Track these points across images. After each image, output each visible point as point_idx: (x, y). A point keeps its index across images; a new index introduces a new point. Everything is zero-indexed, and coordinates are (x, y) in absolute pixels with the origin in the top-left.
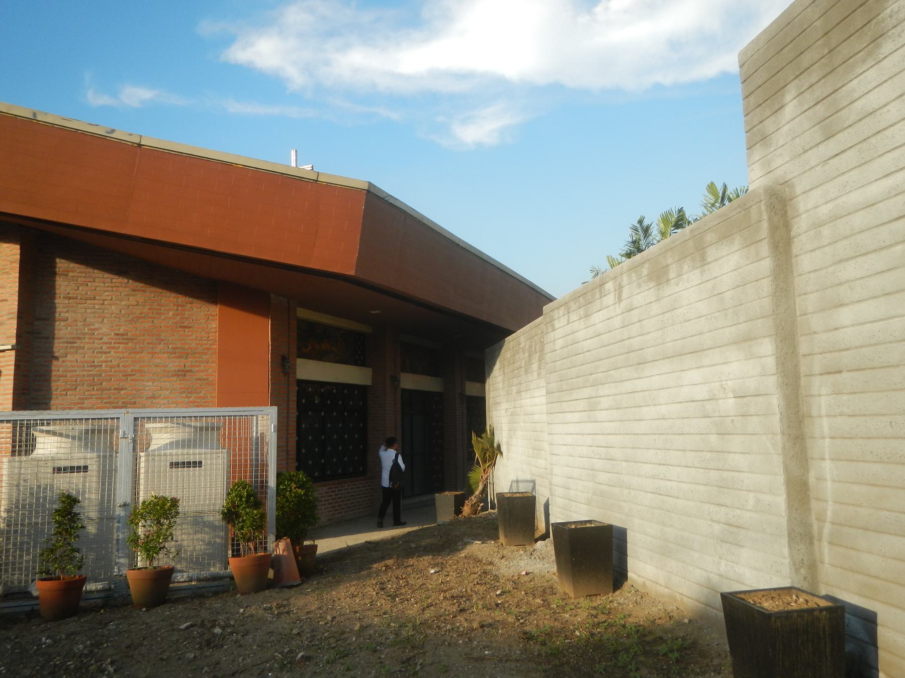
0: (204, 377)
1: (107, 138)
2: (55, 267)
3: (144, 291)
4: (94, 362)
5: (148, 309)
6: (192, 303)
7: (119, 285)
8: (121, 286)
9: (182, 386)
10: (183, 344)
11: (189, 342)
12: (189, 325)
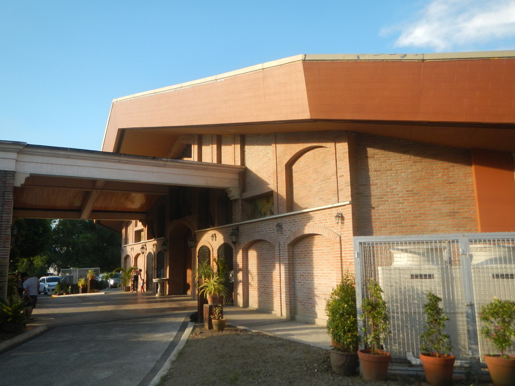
0: (468, 216)
1: (402, 61)
2: (367, 153)
3: (421, 162)
4: (395, 209)
5: (425, 173)
6: (453, 166)
7: (405, 160)
8: (406, 160)
9: (453, 223)
10: (450, 194)
11: (454, 192)
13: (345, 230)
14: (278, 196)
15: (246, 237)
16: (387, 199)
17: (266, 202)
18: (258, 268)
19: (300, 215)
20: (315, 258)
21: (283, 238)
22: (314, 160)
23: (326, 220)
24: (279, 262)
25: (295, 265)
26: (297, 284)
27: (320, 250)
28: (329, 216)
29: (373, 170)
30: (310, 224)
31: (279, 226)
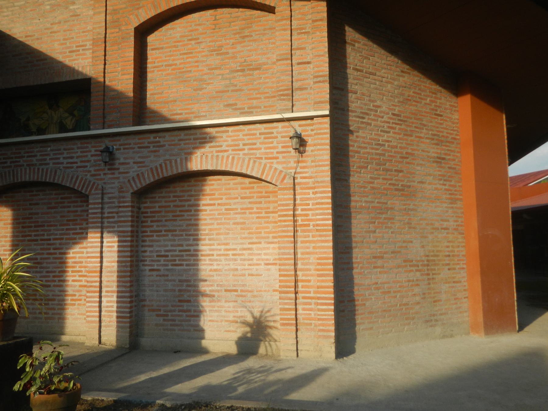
3: (409, 74)
7: (392, 64)
9: (440, 173)
12: (441, 114)
13: (308, 164)
14: (104, 91)
16: (369, 121)
19: (176, 133)
20: (205, 219)
21: (118, 178)
22: (214, 29)
23: (255, 144)
24: (99, 230)
25: (141, 235)
26: (147, 273)
27: (219, 204)
28: (263, 136)
29: (352, 66)
30: (207, 149)
31: (109, 152)
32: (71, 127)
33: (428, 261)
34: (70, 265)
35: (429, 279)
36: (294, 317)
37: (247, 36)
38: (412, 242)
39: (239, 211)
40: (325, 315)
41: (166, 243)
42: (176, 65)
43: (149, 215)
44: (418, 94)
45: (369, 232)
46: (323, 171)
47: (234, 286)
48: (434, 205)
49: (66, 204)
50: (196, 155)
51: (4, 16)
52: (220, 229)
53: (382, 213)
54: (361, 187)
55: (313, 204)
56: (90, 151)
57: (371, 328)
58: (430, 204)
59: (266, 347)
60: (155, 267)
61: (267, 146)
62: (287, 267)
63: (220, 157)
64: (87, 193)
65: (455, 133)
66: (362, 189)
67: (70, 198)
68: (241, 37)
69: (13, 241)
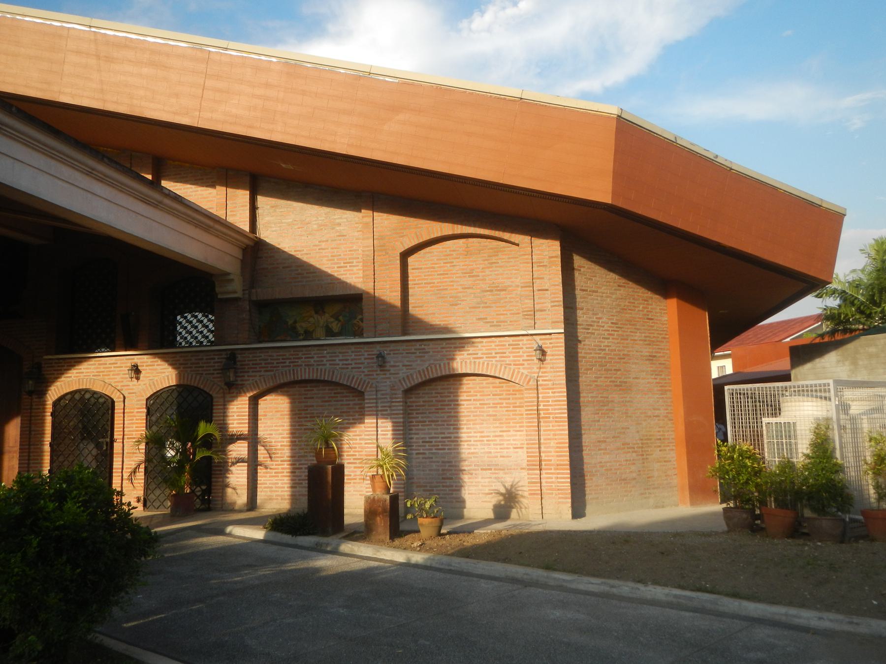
2: (573, 263)
3: (625, 287)
7: (611, 281)
9: (652, 369)
13: (548, 370)
15: (262, 373)
16: (593, 331)
17: (313, 312)
18: (291, 433)
19: (439, 342)
20: (463, 412)
21: (389, 378)
23: (505, 353)
26: (415, 456)
27: (474, 400)
29: (579, 288)
32: (337, 331)
33: (642, 444)
34: (345, 449)
35: (643, 459)
36: (539, 488)
37: (495, 263)
38: (628, 428)
39: (491, 405)
40: (564, 486)
41: (430, 431)
42: (434, 283)
43: (414, 408)
44: (633, 303)
45: (594, 421)
46: (559, 376)
47: (488, 465)
48: (647, 396)
49: (339, 399)
50: (457, 361)
51: (273, 231)
52: (476, 420)
53: (604, 406)
54: (588, 385)
55: (552, 401)
56: (363, 355)
57: (597, 498)
58: (644, 396)
59: (518, 512)
60: (421, 451)
61: (514, 354)
62: (533, 450)
63: (477, 363)
64: (363, 390)
65: (665, 333)
66: (589, 387)
67: (343, 393)
68: (489, 263)
69: (291, 429)
